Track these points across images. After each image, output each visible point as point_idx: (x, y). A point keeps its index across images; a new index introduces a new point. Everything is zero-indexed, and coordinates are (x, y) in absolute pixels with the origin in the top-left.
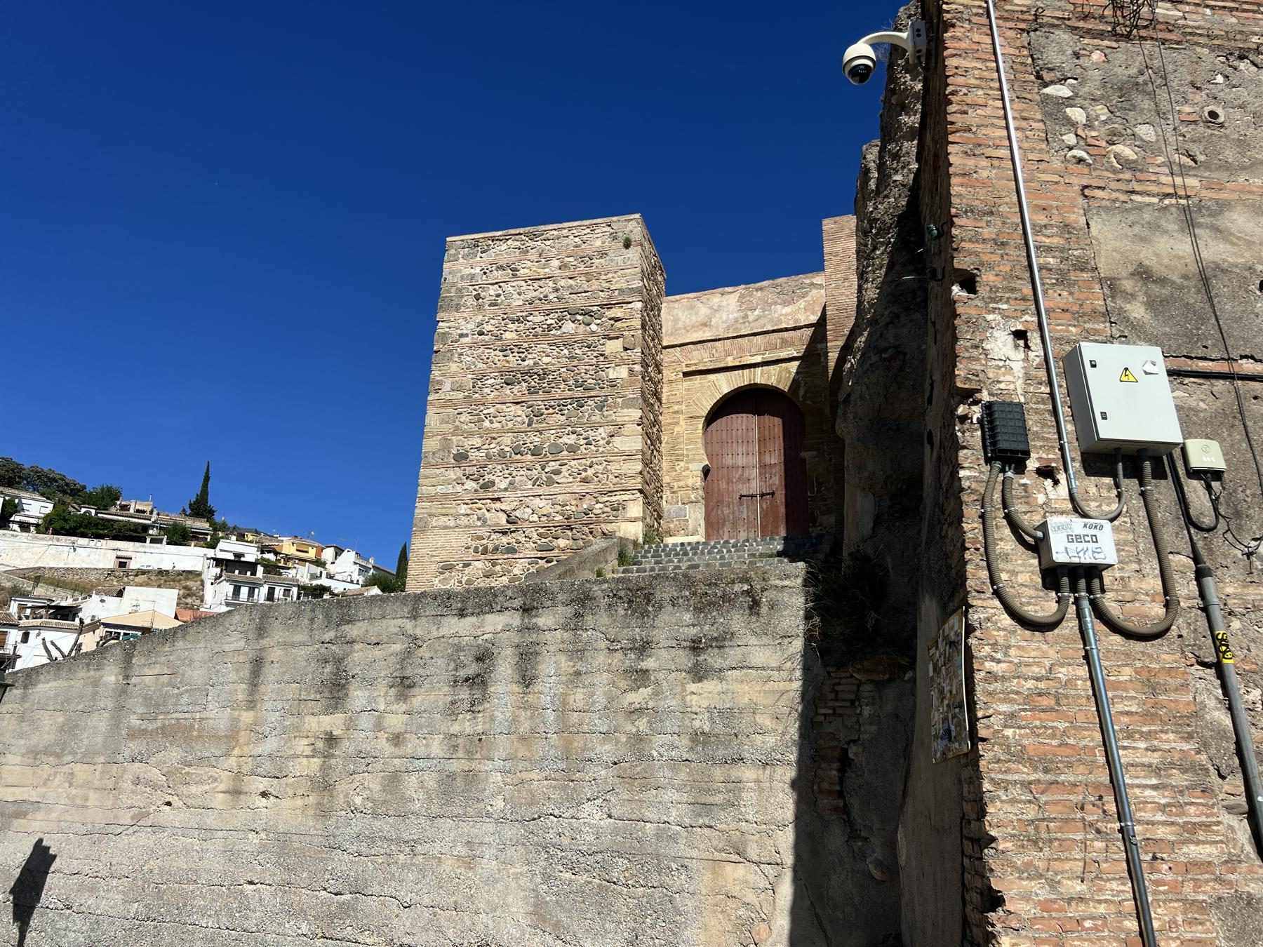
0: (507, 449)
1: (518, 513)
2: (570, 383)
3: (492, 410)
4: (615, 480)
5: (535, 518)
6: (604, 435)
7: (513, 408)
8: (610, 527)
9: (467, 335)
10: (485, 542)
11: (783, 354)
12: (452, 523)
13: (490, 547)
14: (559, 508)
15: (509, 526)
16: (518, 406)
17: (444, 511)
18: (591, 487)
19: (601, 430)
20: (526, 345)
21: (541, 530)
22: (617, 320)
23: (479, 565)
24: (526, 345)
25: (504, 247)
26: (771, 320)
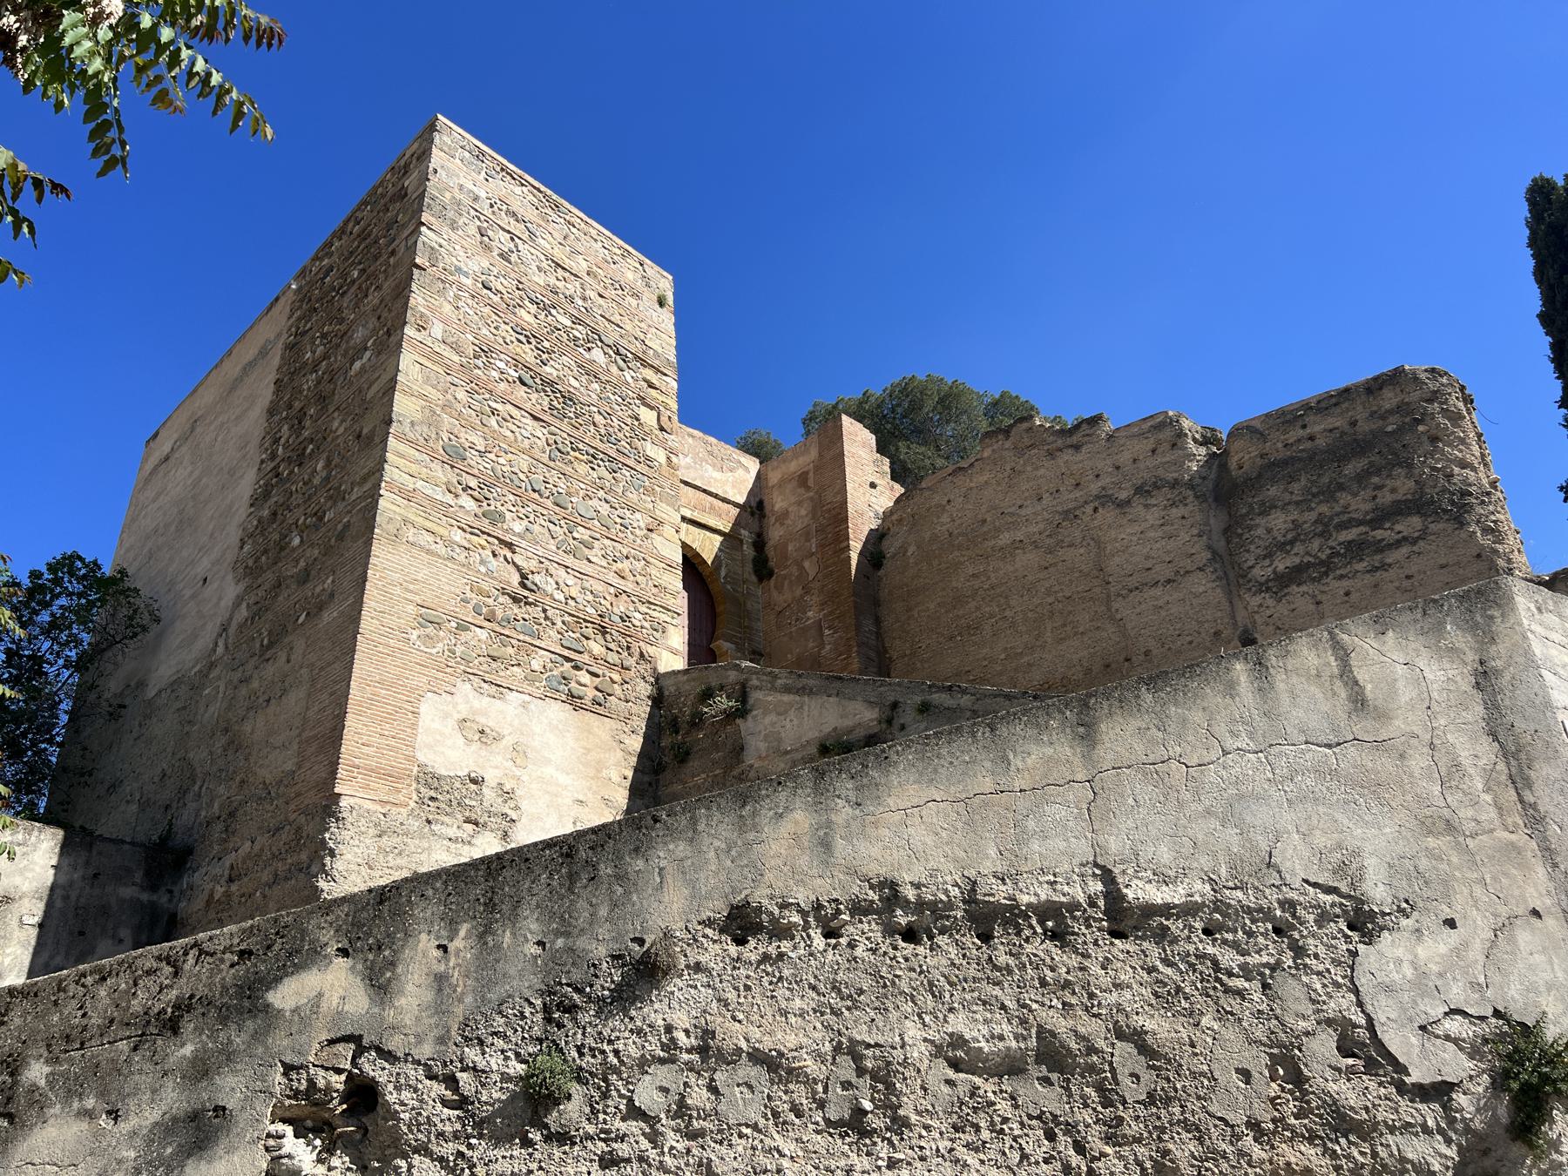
0: (522, 476)
1: (537, 578)
2: (603, 432)
3: (498, 406)
4: (655, 590)
5: (560, 597)
6: (643, 525)
7: (529, 421)
8: (651, 650)
9: (466, 275)
10: (490, 601)
11: (712, 522)
12: (442, 551)
13: (499, 614)
14: (590, 597)
15: (526, 593)
16: (536, 424)
17: (429, 525)
18: (629, 586)
19: (638, 515)
20: (546, 344)
21: (567, 618)
22: (651, 386)
23: (482, 634)
24: (546, 344)
25: (518, 190)
26: (702, 477)
